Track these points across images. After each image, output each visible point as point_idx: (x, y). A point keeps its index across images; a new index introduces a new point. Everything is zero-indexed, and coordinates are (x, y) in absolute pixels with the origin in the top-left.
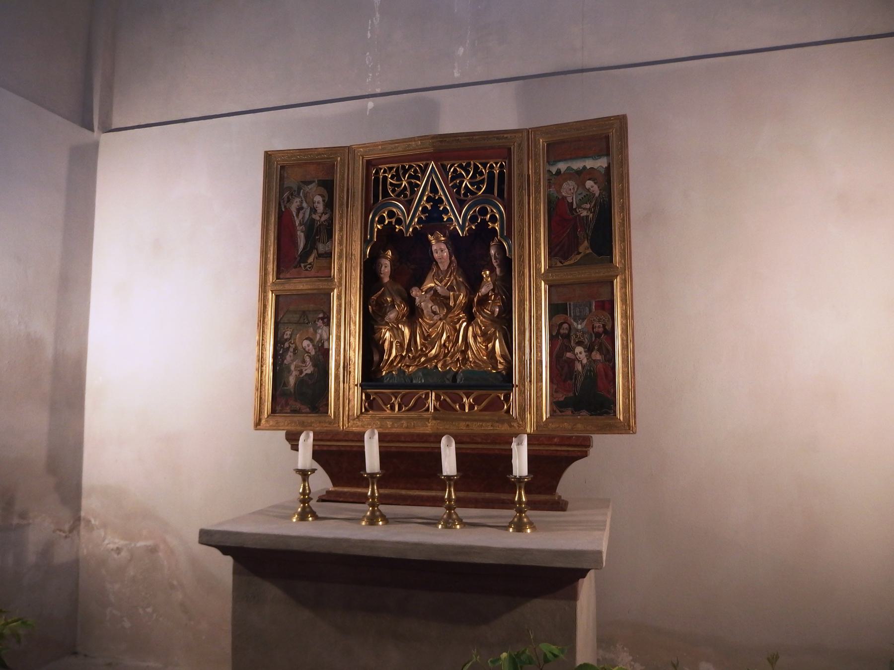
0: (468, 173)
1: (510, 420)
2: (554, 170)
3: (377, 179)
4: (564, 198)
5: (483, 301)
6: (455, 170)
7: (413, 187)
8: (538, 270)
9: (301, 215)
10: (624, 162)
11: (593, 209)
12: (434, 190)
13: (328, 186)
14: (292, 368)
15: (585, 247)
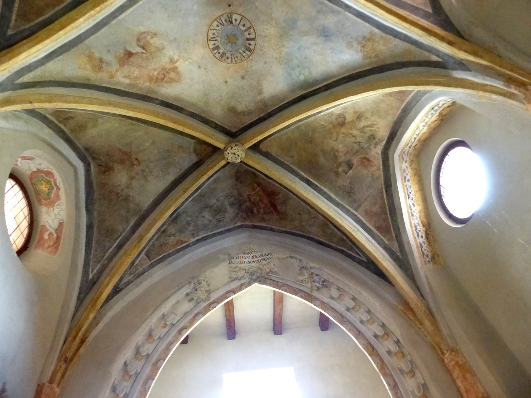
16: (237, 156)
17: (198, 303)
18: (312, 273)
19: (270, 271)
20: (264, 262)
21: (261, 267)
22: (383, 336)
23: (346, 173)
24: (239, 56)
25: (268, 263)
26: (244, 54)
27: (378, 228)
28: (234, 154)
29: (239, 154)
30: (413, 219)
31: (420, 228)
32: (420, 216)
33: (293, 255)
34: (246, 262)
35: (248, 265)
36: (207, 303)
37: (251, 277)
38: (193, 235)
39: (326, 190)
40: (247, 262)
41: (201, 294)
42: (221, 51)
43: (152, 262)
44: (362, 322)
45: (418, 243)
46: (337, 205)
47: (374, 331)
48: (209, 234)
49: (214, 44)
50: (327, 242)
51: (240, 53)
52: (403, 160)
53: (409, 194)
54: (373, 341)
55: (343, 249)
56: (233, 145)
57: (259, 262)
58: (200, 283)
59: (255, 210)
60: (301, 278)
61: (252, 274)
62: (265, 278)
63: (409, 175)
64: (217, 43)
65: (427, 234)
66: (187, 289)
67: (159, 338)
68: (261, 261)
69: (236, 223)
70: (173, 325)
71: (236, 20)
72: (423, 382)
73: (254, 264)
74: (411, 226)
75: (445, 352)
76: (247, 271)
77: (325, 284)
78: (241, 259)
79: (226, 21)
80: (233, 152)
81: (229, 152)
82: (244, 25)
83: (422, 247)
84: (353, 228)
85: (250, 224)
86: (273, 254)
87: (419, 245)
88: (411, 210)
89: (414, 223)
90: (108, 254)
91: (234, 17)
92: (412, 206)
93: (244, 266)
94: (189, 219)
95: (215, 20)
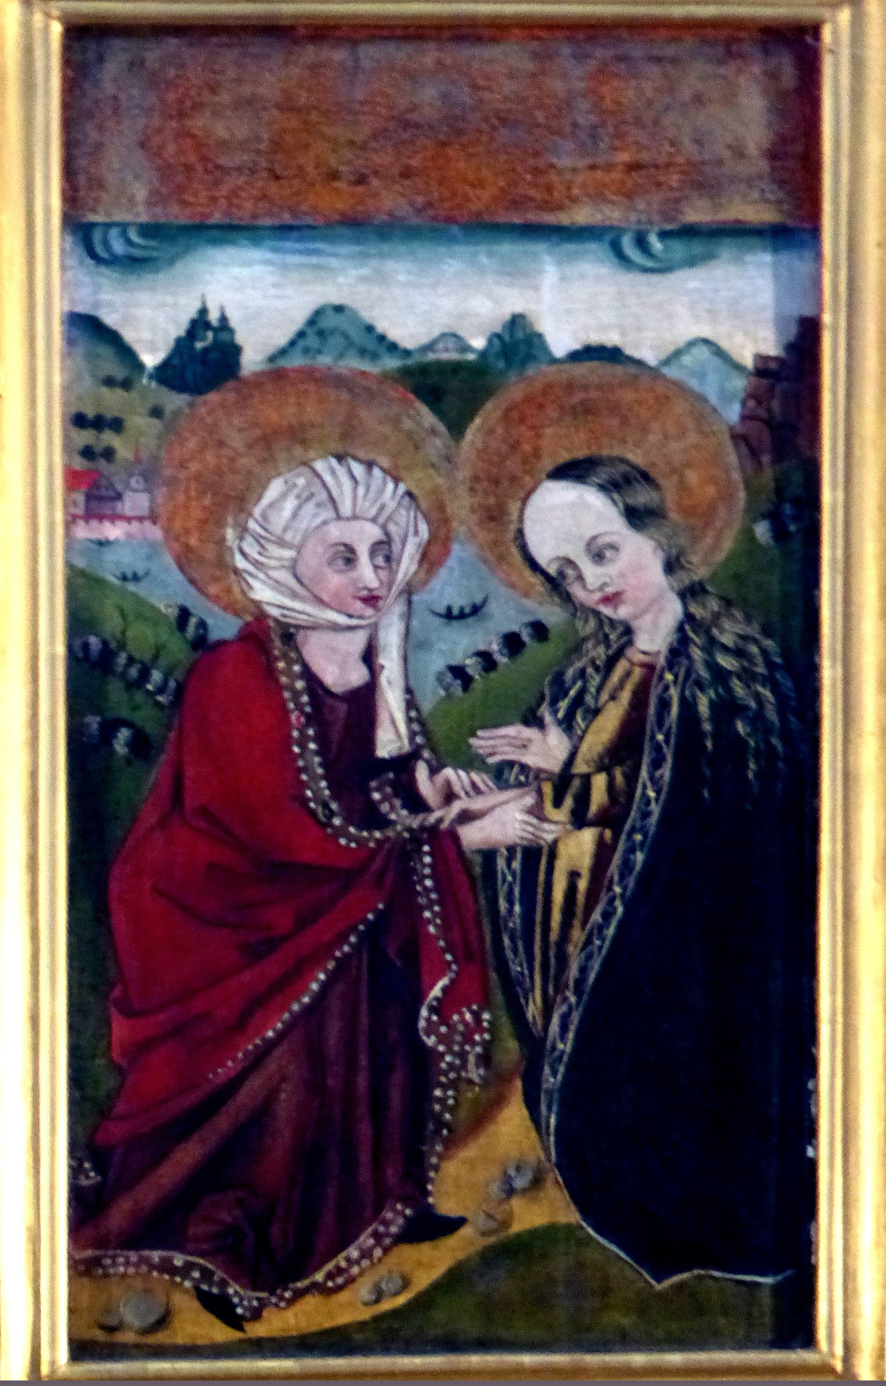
11: (599, 782)
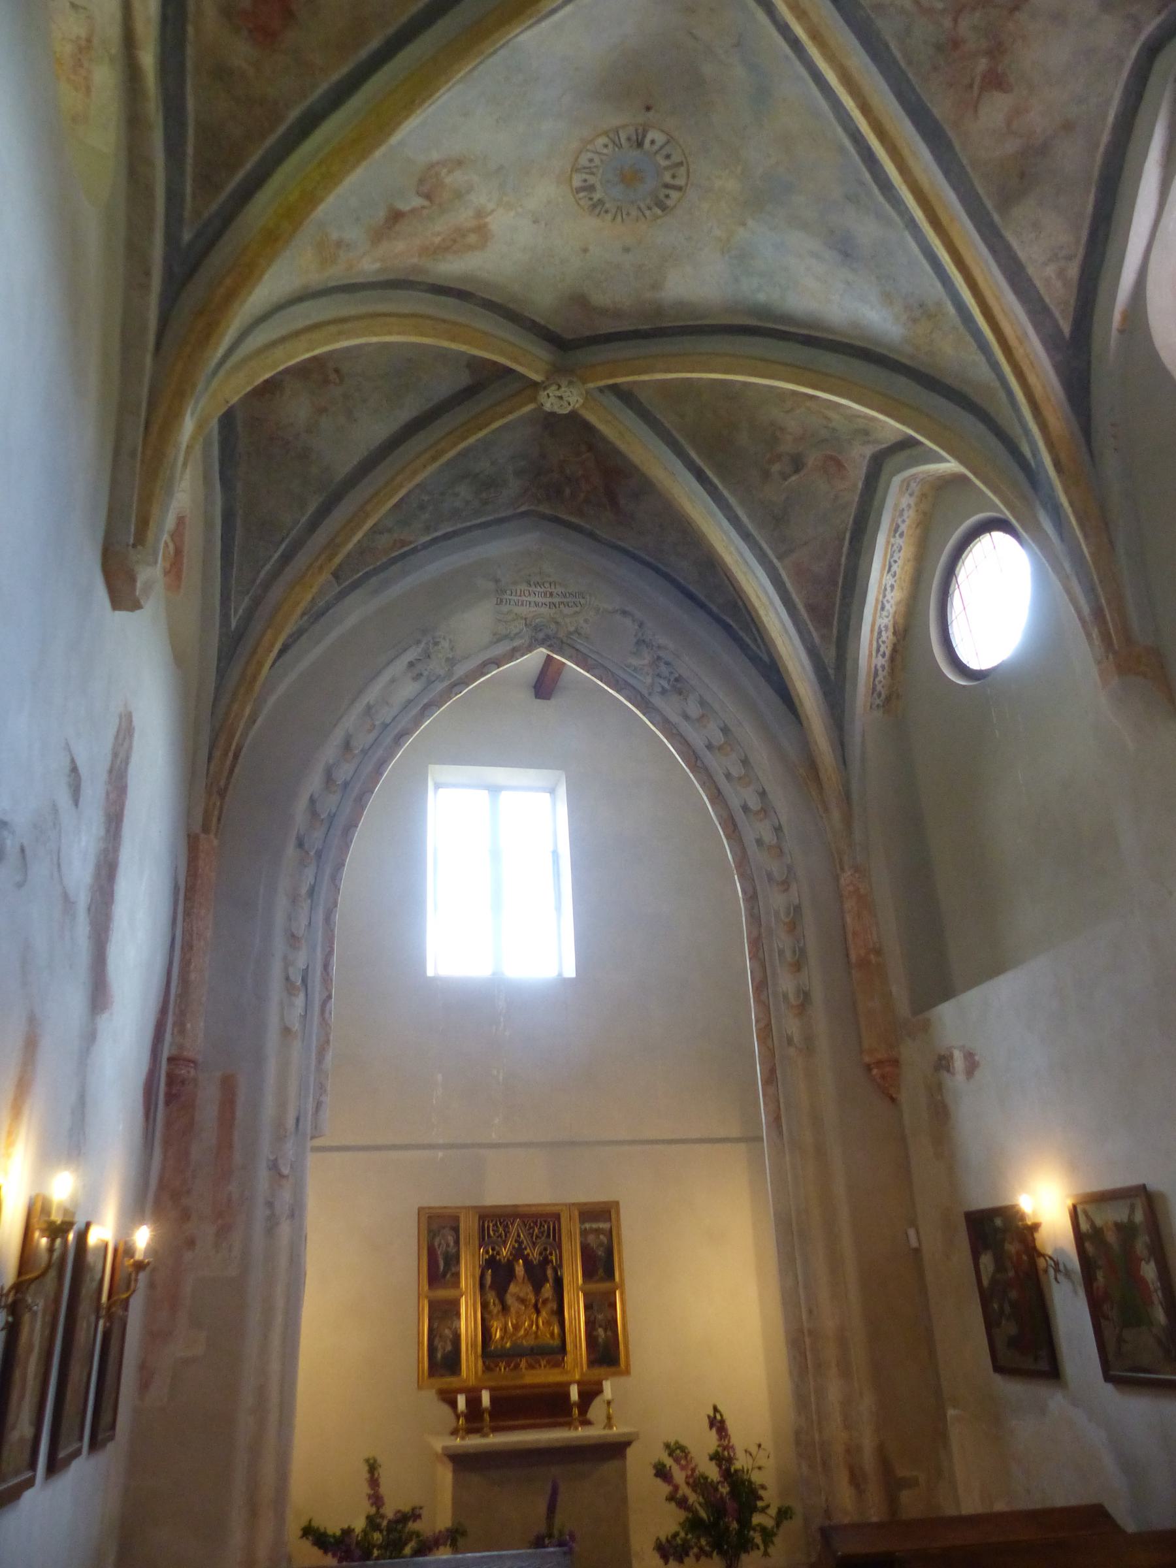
0: (537, 1226)
1: (567, 1372)
2: (583, 1227)
3: (483, 1226)
4: (589, 1244)
5: (545, 1302)
6: (530, 1225)
7: (507, 1233)
8: (577, 1284)
9: (441, 1248)
10: (619, 1227)
12: (519, 1236)
13: (456, 1230)
14: (439, 1346)
15: (601, 1272)
16: (565, 404)
17: (430, 682)
18: (659, 658)
19: (577, 631)
20: (566, 611)
21: (560, 620)
22: (757, 813)
23: (785, 479)
24: (634, 213)
25: (576, 613)
26: (648, 213)
27: (811, 609)
28: (561, 398)
29: (570, 400)
30: (880, 617)
31: (888, 637)
32: (895, 612)
33: (627, 609)
34: (530, 603)
35: (532, 609)
36: (446, 683)
37: (534, 634)
38: (427, 529)
39: (732, 500)
40: (532, 604)
41: (436, 666)
42: (597, 196)
43: (342, 586)
44: (728, 776)
45: (873, 666)
46: (746, 536)
47: (745, 799)
48: (459, 526)
49: (585, 181)
50: (703, 598)
51: (639, 208)
52: (907, 490)
53: (893, 563)
54: (740, 816)
55: (732, 623)
56: (564, 383)
57: (555, 606)
58: (436, 644)
59: (568, 491)
60: (634, 662)
61: (537, 629)
62: (562, 642)
63: (908, 522)
64: (592, 180)
65: (895, 650)
66: (411, 655)
67: (362, 751)
68: (561, 606)
69: (519, 507)
70: (385, 726)
71: (653, 142)
72: (797, 902)
73: (544, 610)
74: (872, 631)
75: (846, 868)
76: (528, 622)
77: (679, 685)
78: (520, 596)
79: (629, 139)
80: (560, 395)
81: (551, 394)
82: (668, 157)
83: (876, 674)
84: (764, 599)
85: (548, 512)
86: (588, 597)
87: (873, 669)
88: (884, 596)
89: (880, 625)
90: (263, 574)
91: (650, 136)
92: (889, 589)
93: (523, 610)
94: (426, 498)
95: (606, 133)
